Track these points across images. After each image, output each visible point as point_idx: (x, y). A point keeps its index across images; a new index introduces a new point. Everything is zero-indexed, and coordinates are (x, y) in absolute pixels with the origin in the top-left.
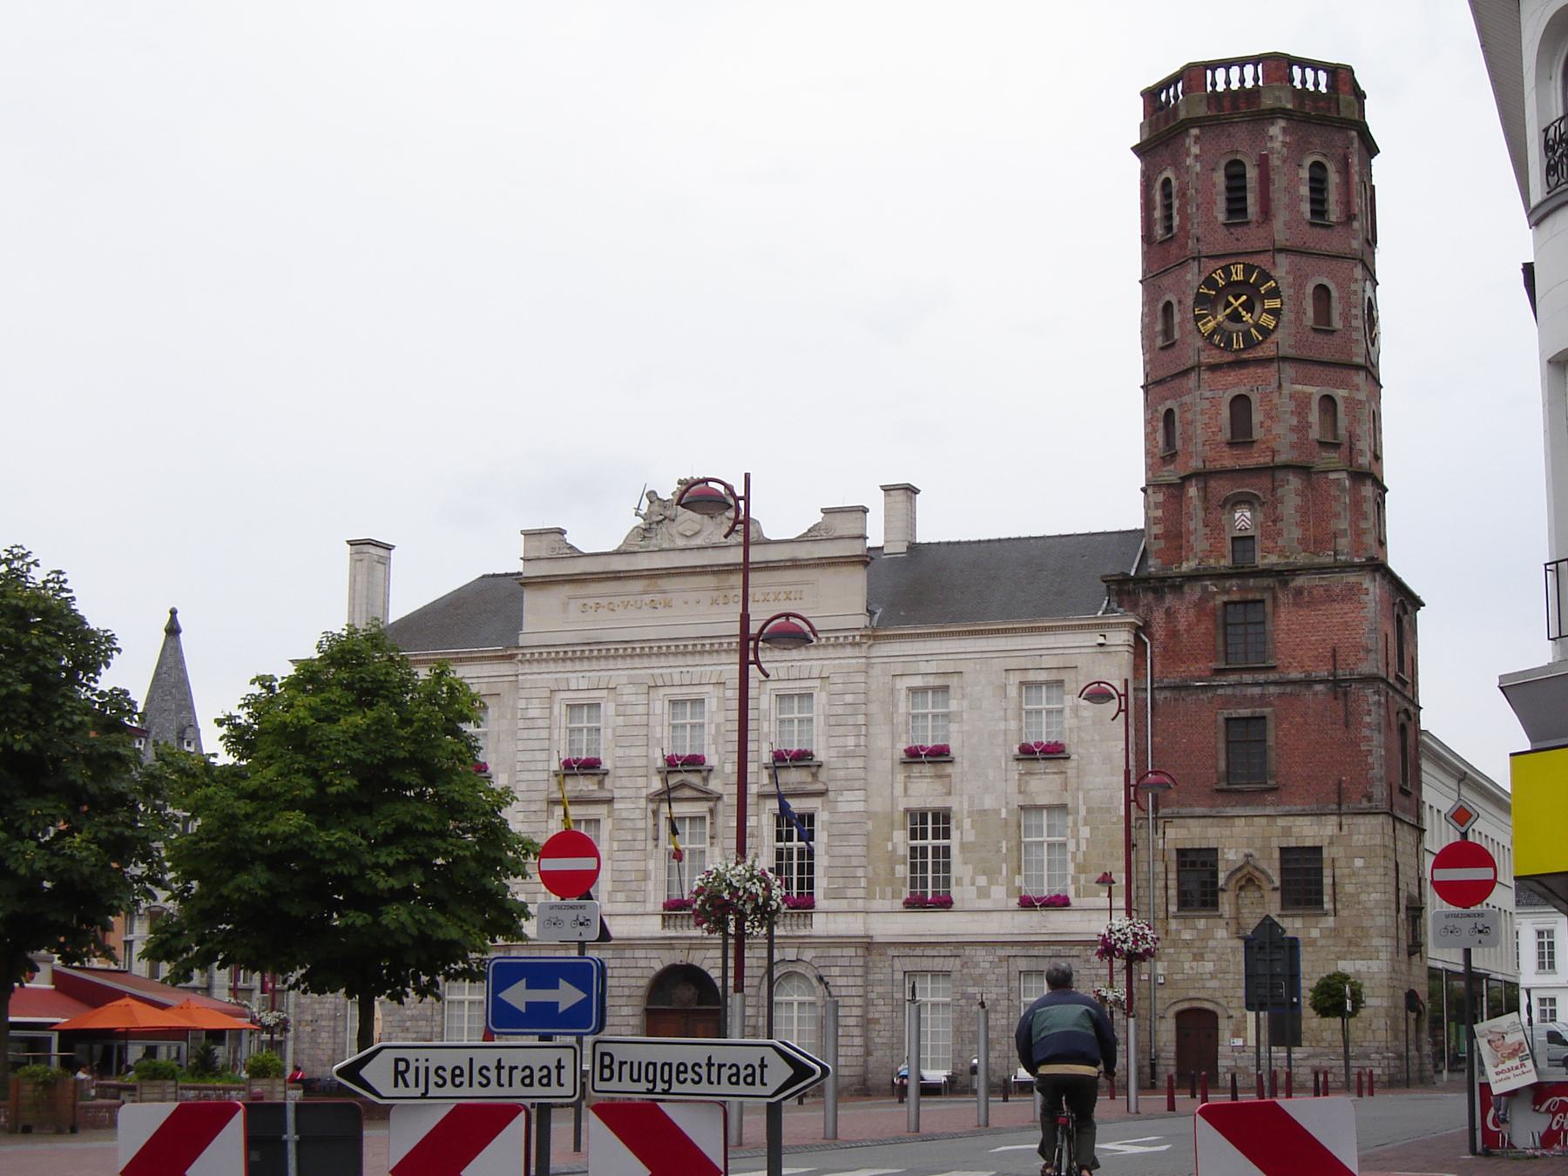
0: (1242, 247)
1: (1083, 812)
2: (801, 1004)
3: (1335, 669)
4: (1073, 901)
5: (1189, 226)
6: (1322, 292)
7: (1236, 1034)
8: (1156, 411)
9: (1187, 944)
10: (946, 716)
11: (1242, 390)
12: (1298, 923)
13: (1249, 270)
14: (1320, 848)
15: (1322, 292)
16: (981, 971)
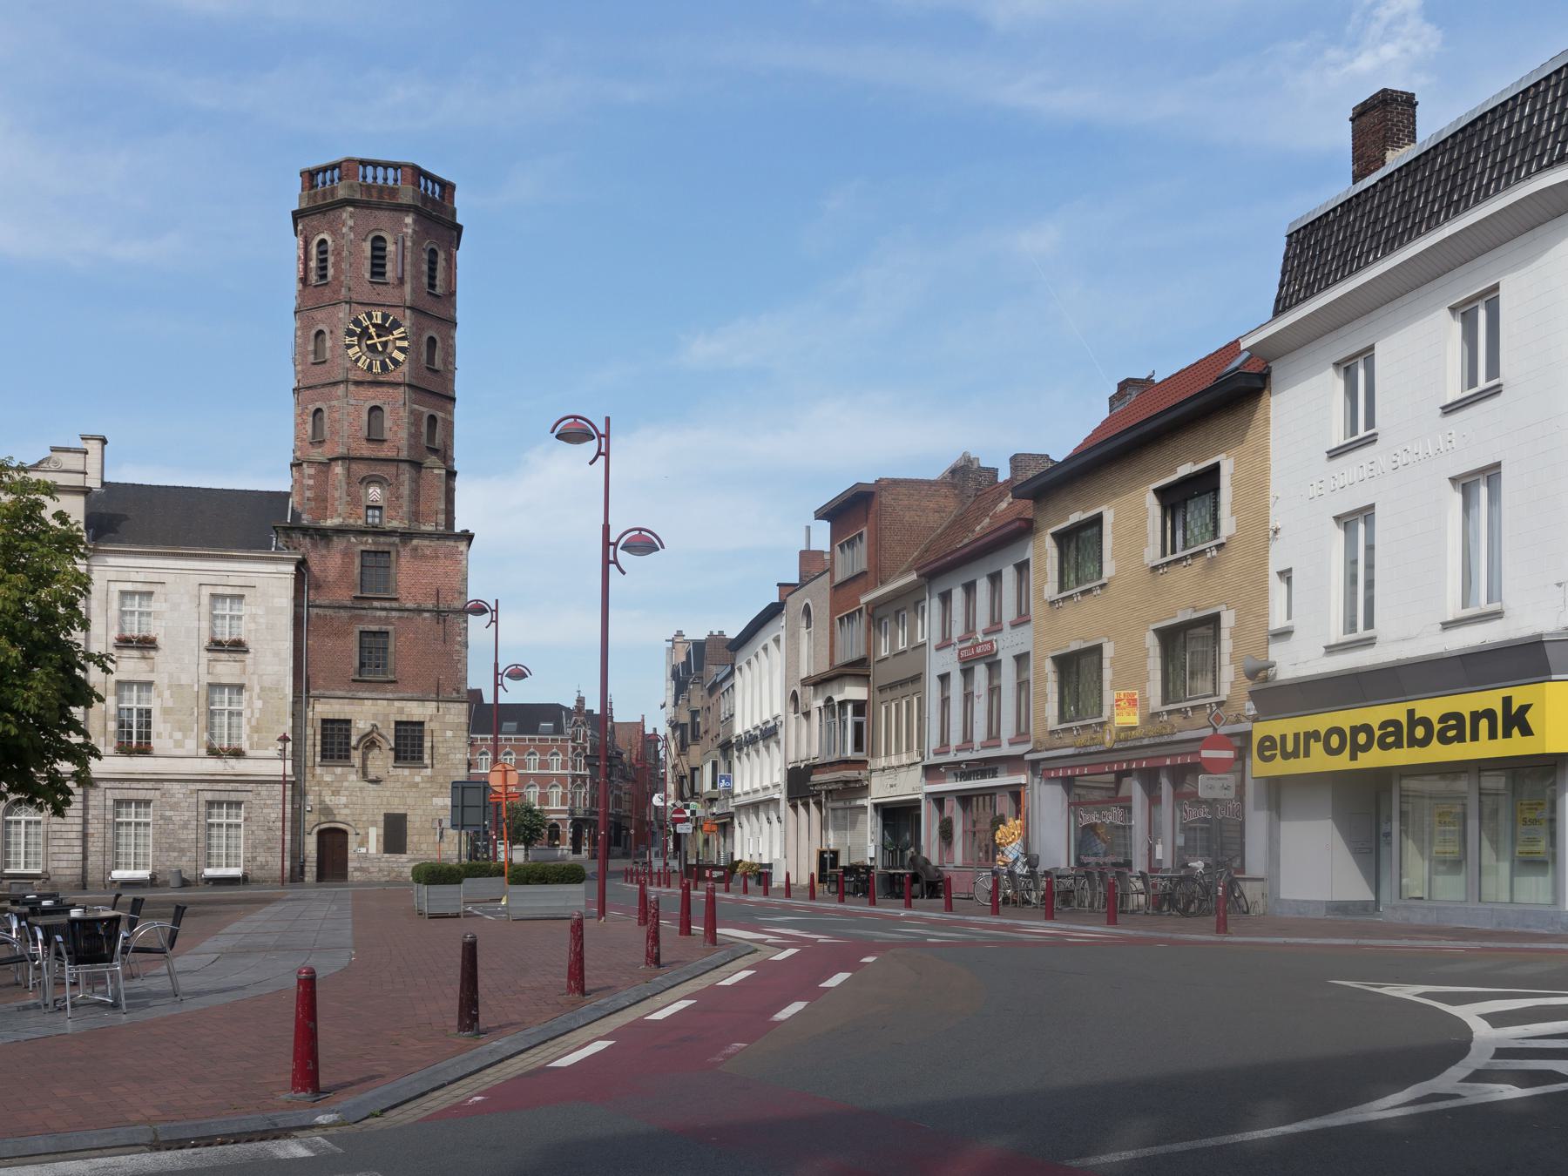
0: (381, 300)
1: (257, 689)
2: (28, 823)
3: (438, 603)
4: (250, 753)
5: (343, 278)
6: (432, 341)
7: (361, 845)
8: (307, 408)
9: (328, 784)
10: (149, 614)
11: (377, 403)
12: (406, 772)
13: (385, 317)
14: (421, 724)
15: (432, 341)
16: (176, 800)
